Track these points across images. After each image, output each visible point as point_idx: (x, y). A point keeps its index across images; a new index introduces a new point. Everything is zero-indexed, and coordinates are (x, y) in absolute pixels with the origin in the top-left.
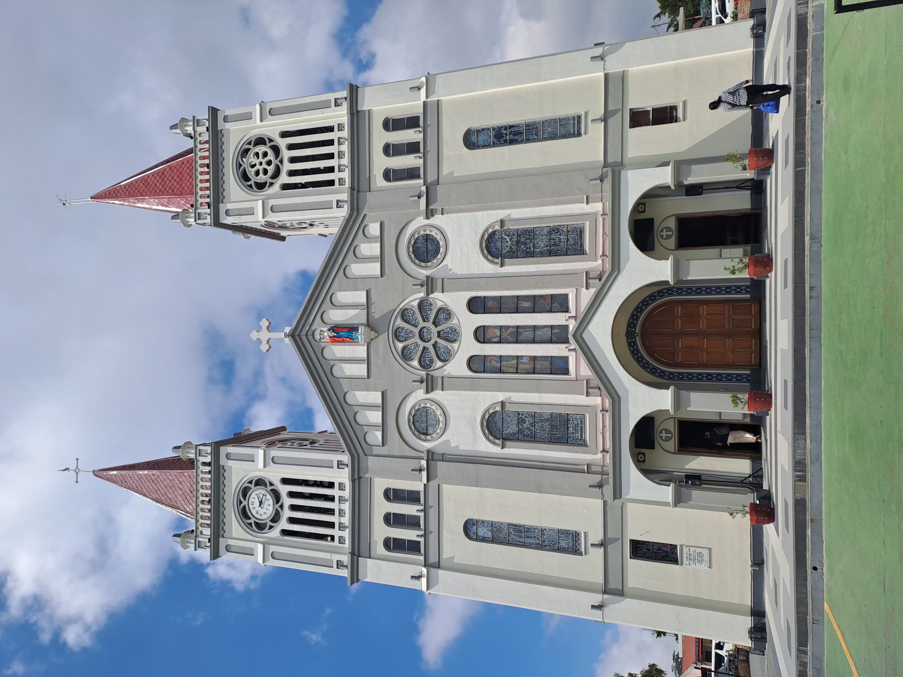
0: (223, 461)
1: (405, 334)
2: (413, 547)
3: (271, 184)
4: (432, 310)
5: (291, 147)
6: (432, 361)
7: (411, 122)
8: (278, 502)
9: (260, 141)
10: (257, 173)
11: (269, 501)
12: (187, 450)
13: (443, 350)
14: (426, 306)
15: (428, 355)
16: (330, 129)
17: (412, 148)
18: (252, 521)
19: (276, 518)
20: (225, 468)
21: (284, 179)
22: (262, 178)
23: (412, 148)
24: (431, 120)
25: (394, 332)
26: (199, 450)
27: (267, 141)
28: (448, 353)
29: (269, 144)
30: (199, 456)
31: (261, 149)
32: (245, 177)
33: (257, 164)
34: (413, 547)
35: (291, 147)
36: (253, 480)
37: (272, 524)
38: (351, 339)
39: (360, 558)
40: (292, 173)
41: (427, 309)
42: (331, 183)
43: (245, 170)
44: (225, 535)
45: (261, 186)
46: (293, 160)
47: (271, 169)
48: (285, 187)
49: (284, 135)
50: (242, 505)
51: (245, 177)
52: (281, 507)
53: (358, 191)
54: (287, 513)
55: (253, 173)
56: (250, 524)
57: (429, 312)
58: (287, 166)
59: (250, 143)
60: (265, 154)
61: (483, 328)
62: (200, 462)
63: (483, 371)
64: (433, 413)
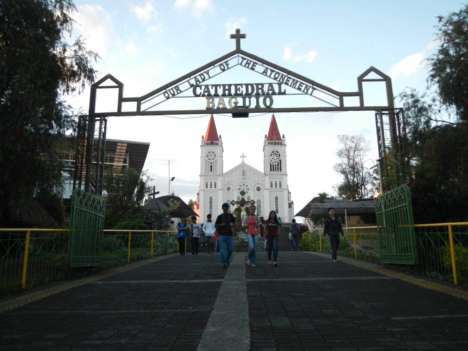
0: (219, 148)
2: (207, 187)
7: (280, 186)
9: (279, 155)
16: (281, 170)
17: (276, 187)
18: (208, 154)
19: (209, 159)
21: (273, 160)
23: (276, 187)
32: (273, 152)
34: (207, 187)
42: (271, 170)
49: (280, 161)
51: (273, 152)
54: (210, 161)
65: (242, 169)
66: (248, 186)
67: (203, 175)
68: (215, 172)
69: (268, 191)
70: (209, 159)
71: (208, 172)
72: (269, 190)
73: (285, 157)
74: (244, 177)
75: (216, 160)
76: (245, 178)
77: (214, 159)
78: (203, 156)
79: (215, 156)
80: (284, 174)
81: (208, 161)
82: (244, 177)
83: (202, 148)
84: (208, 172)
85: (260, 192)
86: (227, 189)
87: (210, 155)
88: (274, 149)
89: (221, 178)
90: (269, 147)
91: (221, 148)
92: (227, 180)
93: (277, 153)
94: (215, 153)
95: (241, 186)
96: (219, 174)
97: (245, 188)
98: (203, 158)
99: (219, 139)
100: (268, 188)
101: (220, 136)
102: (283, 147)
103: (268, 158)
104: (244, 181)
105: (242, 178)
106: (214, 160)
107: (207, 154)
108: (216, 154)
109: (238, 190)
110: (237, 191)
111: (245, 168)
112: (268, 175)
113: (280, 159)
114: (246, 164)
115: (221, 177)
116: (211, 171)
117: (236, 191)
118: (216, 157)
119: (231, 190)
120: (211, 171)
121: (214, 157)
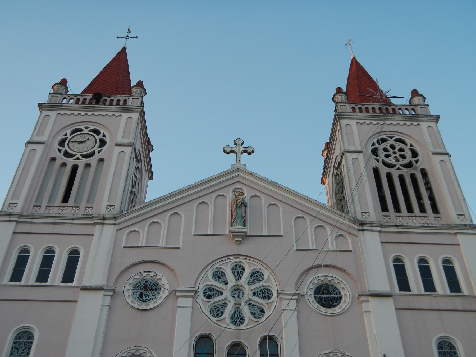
0: (125, 116)
1: (238, 272)
3: (378, 161)
4: (264, 299)
5: (413, 177)
6: (209, 297)
8: (85, 156)
9: (415, 154)
10: (385, 150)
11: (86, 148)
12: (139, 90)
13: (221, 309)
14: (268, 293)
15: (216, 294)
16: (435, 209)
18: (69, 137)
19: (67, 154)
20: (120, 117)
21: (384, 171)
22: (382, 155)
24: (458, 303)
25: (241, 260)
26: (139, 99)
27: (416, 159)
28: (218, 315)
29: (413, 160)
30: (133, 99)
31: (408, 154)
33: (394, 151)
35: (413, 177)
36: (106, 137)
37: (62, 152)
38: (235, 218)
39: (15, 224)
40: (389, 176)
41: (264, 294)
42: (384, 208)
43: (386, 141)
44: (59, 115)
45: (375, 152)
46: (401, 178)
47: (391, 160)
48: (376, 171)
50: (84, 129)
52: (78, 159)
53: (380, 231)
54: (71, 162)
55: (385, 146)
56: (66, 135)
57: (261, 296)
58: (395, 174)
59: (411, 145)
60: (403, 157)
61: (244, 353)
62: (128, 99)
63: (196, 352)
64: (154, 298)
65: (230, 196)
66: (266, 274)
67: (10, 215)
68: (83, 204)
69: (389, 303)
70: (67, 154)
71: (44, 203)
72: (390, 300)
73: (445, 158)
74: (238, 228)
75: (101, 160)
76: (245, 237)
77: (93, 153)
78: (44, 138)
79: (103, 143)
80: (458, 221)
81: (61, 158)
82: (238, 228)
83: (45, 113)
84: (44, 203)
85: (337, 310)
86: (137, 288)
87: (80, 138)
88: (386, 128)
89: (109, 230)
90: (361, 122)
91: (136, 116)
92: (142, 243)
93: (398, 145)
94: (102, 131)
95: (219, 275)
96: (103, 211)
97: (248, 290)
98: (40, 148)
99: (134, 90)
100: (384, 287)
101: (140, 84)
102: (424, 125)
103: (360, 157)
104: (244, 249)
105: (233, 235)
106: (93, 161)
107: (61, 137)
108: (107, 139)
109: (201, 296)
110: (194, 298)
111: (247, 194)
112: (372, 224)
113: (420, 165)
114: (251, 174)
115: (116, 227)
116: (66, 199)
117: (189, 302)
118: (104, 148)
119: (164, 294)
120: (66, 199)
121: (96, 149)
